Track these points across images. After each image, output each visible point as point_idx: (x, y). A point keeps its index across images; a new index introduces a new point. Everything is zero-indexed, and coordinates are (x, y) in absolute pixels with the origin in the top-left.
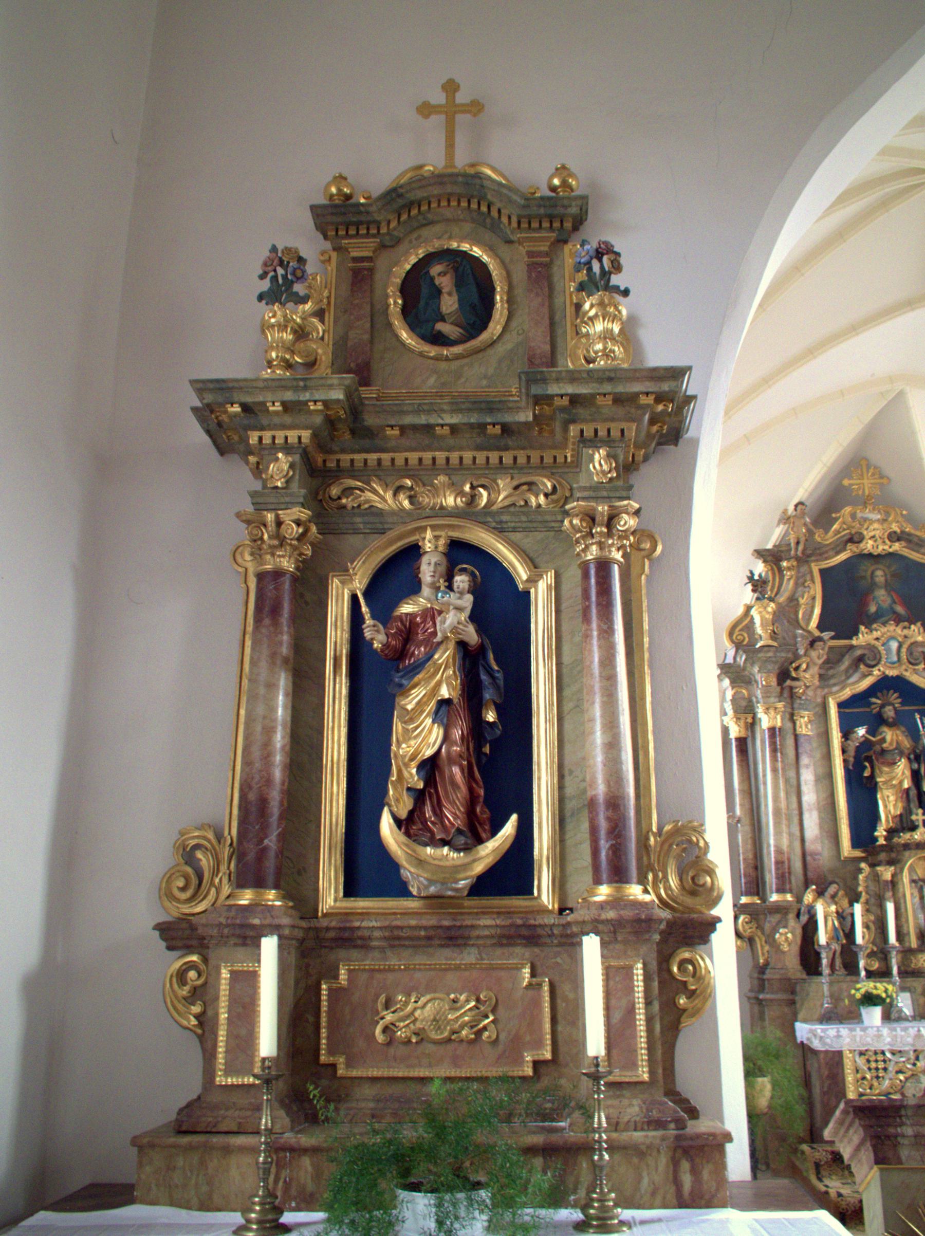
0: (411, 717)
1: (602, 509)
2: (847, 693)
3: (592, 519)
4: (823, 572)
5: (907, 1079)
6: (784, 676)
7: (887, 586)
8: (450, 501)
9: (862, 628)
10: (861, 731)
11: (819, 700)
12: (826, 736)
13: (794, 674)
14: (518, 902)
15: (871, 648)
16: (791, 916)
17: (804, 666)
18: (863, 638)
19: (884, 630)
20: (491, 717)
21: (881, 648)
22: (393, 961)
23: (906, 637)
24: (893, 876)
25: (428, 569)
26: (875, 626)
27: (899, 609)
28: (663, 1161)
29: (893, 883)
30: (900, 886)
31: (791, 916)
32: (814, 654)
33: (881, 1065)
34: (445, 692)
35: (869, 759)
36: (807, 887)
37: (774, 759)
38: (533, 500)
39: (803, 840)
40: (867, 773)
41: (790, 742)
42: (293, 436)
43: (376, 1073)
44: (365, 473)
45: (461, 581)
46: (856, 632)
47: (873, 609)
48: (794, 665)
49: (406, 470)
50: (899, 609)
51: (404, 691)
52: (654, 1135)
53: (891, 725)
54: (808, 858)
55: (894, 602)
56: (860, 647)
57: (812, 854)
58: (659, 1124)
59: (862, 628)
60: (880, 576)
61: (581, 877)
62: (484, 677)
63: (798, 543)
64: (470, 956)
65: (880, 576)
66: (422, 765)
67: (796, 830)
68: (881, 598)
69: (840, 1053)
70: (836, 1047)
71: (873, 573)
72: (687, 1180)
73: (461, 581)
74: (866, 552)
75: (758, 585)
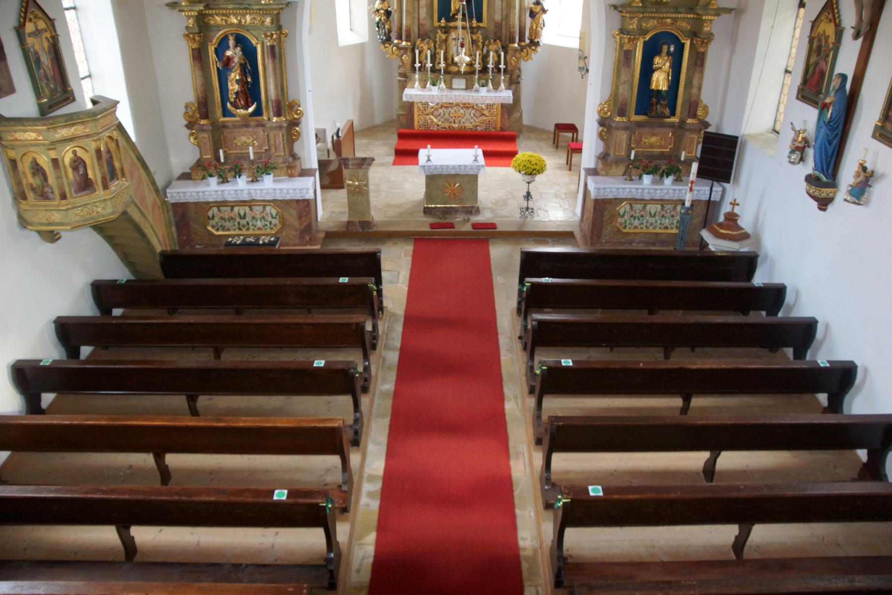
0: (231, 81)
1: (269, 34)
3: (266, 36)
8: (235, 21)
14: (260, 118)
20: (249, 80)
22: (235, 131)
24: (446, 37)
25: (231, 42)
28: (285, 170)
29: (446, 40)
30: (448, 43)
31: (409, 51)
33: (426, 106)
34: (238, 78)
36: (419, 38)
38: (256, 22)
39: (419, 19)
42: (193, 13)
43: (234, 152)
44: (212, 15)
45: (239, 49)
49: (223, 15)
51: (230, 75)
52: (283, 165)
58: (285, 163)
61: (271, 114)
62: (247, 71)
64: (250, 129)
66: (235, 93)
67: (416, 15)
69: (413, 103)
70: (411, 100)
72: (289, 172)
73: (239, 49)
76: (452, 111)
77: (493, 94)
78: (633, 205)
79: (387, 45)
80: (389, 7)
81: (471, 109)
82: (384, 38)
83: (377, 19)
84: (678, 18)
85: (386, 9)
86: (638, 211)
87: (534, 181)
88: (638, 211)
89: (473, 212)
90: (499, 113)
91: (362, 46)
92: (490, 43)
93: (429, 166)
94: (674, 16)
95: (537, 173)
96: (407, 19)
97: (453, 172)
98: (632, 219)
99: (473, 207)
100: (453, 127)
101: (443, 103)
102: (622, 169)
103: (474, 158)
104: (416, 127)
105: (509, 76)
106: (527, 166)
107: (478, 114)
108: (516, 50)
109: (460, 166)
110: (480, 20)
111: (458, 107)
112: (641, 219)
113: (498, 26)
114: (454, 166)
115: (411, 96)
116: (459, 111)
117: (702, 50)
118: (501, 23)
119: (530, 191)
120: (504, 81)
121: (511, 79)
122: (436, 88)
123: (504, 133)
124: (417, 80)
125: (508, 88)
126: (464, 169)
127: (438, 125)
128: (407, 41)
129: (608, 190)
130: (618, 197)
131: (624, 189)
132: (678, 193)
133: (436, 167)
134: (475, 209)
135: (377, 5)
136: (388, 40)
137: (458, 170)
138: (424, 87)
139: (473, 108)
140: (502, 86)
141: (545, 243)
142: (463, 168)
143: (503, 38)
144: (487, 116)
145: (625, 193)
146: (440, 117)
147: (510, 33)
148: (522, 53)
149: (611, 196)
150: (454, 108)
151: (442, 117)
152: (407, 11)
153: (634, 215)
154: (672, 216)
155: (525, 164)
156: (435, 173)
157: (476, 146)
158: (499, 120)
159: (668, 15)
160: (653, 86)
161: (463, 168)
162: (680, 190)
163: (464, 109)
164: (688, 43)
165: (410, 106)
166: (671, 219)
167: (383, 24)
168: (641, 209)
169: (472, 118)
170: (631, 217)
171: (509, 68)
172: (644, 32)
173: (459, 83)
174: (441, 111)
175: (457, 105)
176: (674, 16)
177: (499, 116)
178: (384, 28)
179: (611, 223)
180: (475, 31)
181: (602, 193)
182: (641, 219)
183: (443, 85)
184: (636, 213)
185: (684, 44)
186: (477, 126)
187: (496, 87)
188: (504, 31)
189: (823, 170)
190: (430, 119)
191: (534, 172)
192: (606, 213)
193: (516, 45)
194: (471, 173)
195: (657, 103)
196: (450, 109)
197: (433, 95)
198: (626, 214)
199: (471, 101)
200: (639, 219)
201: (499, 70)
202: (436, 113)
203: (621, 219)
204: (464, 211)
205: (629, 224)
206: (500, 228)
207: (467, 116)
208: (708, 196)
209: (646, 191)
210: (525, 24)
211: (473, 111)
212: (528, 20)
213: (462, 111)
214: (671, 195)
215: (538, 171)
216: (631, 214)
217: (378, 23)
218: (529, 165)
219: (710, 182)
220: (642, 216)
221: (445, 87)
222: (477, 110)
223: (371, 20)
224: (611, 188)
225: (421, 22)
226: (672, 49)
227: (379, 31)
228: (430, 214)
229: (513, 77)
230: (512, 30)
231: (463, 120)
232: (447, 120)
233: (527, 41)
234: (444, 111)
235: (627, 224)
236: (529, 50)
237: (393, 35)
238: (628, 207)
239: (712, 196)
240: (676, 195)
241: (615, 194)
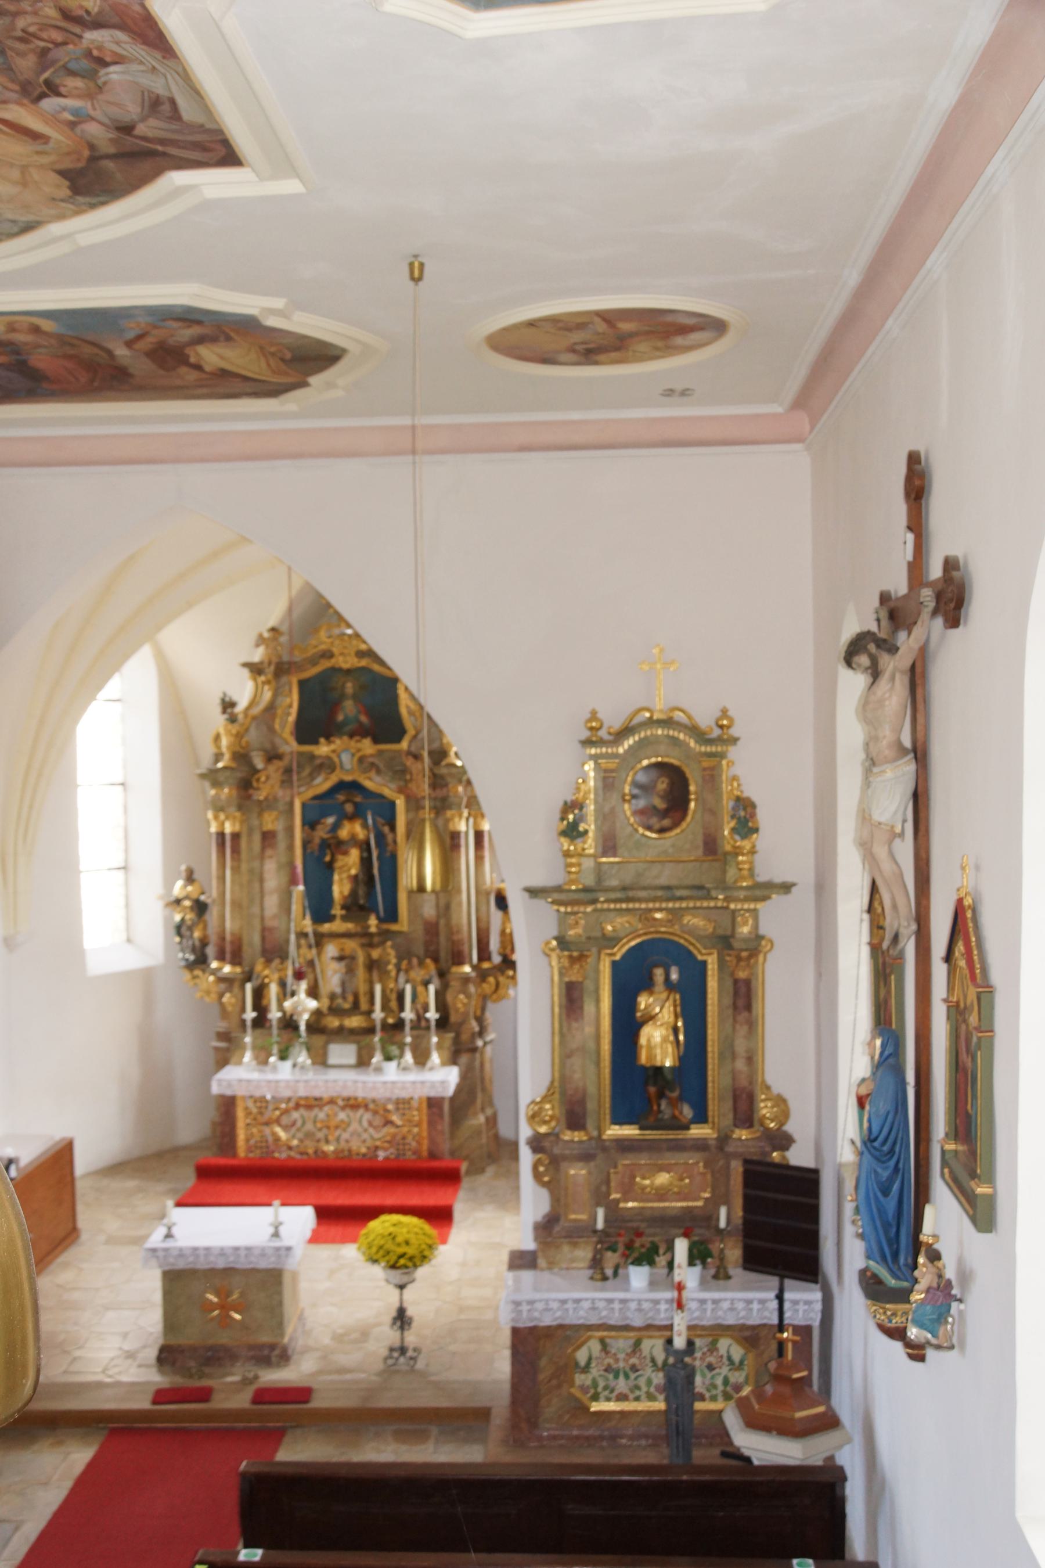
2: (311, 793)
4: (302, 684)
5: (282, 1114)
6: (246, 785)
7: (355, 697)
9: (322, 740)
10: (330, 820)
11: (288, 799)
12: (290, 830)
13: (255, 784)
15: (328, 758)
16: (236, 985)
17: (263, 779)
18: (323, 749)
19: (338, 742)
21: (336, 759)
23: (359, 750)
26: (332, 739)
27: (364, 719)
32: (271, 769)
35: (329, 846)
37: (233, 858)
39: (262, 918)
40: (328, 858)
41: (257, 838)
46: (316, 742)
47: (340, 717)
48: (256, 776)
50: (364, 719)
53: (351, 818)
54: (267, 933)
55: (359, 712)
56: (320, 757)
57: (271, 930)
59: (322, 740)
60: (349, 687)
63: (270, 663)
65: (349, 687)
67: (256, 910)
68: (349, 709)
71: (343, 687)
74: (337, 666)
75: (228, 705)
76: (322, 1115)
77: (414, 1076)
78: (608, 1341)
79: (197, 972)
80: (203, 893)
81: (361, 1111)
82: (192, 958)
83: (178, 918)
84: (681, 909)
85: (195, 896)
86: (621, 1356)
87: (413, 1281)
88: (621, 1356)
89: (274, 1359)
90: (425, 1118)
91: (146, 976)
92: (410, 967)
93: (166, 1250)
94: (670, 905)
95: (410, 1264)
96: (233, 918)
97: (221, 1264)
98: (611, 1376)
99: (272, 1347)
100: (323, 1152)
101: (301, 1098)
102: (584, 1253)
103: (271, 1230)
104: (242, 1151)
105: (451, 1035)
106: (385, 1247)
107: (378, 1121)
108: (466, 980)
109: (236, 1249)
110: (392, 915)
111: (336, 1109)
112: (633, 1376)
113: (432, 930)
114: (222, 1249)
115: (230, 1085)
116: (336, 1114)
117: (742, 975)
118: (437, 924)
119: (405, 1305)
120: (439, 1046)
121: (456, 1041)
122: (288, 1064)
123: (435, 1164)
124: (249, 1046)
125: (453, 1059)
126: (246, 1256)
127: (290, 1148)
128: (234, 963)
129: (540, 1306)
130: (567, 1322)
131: (577, 1301)
132: (713, 1310)
133: (181, 1253)
134: (277, 1352)
135: (179, 888)
136: (200, 961)
137: (232, 1259)
138: (262, 1061)
139: (366, 1107)
140: (435, 1058)
141: (420, 1437)
142: (243, 1253)
143: (443, 954)
144: (397, 1127)
145: (582, 1313)
146: (293, 1130)
147: (453, 943)
148: (485, 985)
149: (547, 1321)
150: (326, 1108)
151: (298, 1130)
152: (234, 903)
153: (615, 1366)
154: (710, 1367)
155: (382, 1242)
156: (181, 1265)
157: (277, 1203)
158: (425, 1134)
159: (657, 905)
160: (643, 1059)
161: (243, 1253)
162: (715, 1302)
163: (348, 1111)
164: (712, 962)
165: (228, 1105)
166: (709, 1375)
167: (190, 929)
168: (629, 1351)
169: (366, 1130)
170: (606, 1370)
171: (453, 1018)
172: (611, 941)
173: (342, 1053)
174: (295, 1115)
175: (332, 1101)
176: (670, 905)
177: (425, 1126)
178: (191, 937)
179: (559, 1386)
180: (376, 940)
181: (525, 1314)
182: (633, 1376)
183: (303, 1058)
184: (617, 1360)
185: (704, 963)
186: (377, 1148)
187: (421, 1059)
188: (442, 939)
189: (884, 1258)
190: (274, 1134)
191: (402, 1261)
192: (543, 1362)
193: (467, 969)
194: (263, 1264)
195: (661, 1095)
196: (316, 1111)
197: (277, 1082)
198: (593, 1365)
199: (360, 1094)
200: (627, 1377)
201: (400, 1025)
202: (285, 1120)
203: (583, 1376)
204: (253, 1358)
206: (317, 1403)
207: (354, 1126)
209: (633, 1305)
210: (488, 923)
211: (367, 1116)
212: (496, 915)
213: (342, 1116)
214: (743, 1314)
215: (411, 1259)
217: (179, 929)
218: (390, 1246)
219: (774, 1281)
220: (634, 1368)
221: (309, 1062)
222: (375, 1113)
223: (167, 919)
224: (547, 1301)
225: (269, 923)
226: (674, 976)
227: (180, 943)
228: (173, 1364)
229: (465, 1037)
230: (455, 938)
231: (345, 1136)
232: (309, 1135)
233: (497, 959)
234: (302, 1116)
235: (600, 1389)
236: (501, 979)
237: (210, 951)
238: (595, 1346)
239: (787, 1315)
240: (709, 1313)
241: (558, 1314)
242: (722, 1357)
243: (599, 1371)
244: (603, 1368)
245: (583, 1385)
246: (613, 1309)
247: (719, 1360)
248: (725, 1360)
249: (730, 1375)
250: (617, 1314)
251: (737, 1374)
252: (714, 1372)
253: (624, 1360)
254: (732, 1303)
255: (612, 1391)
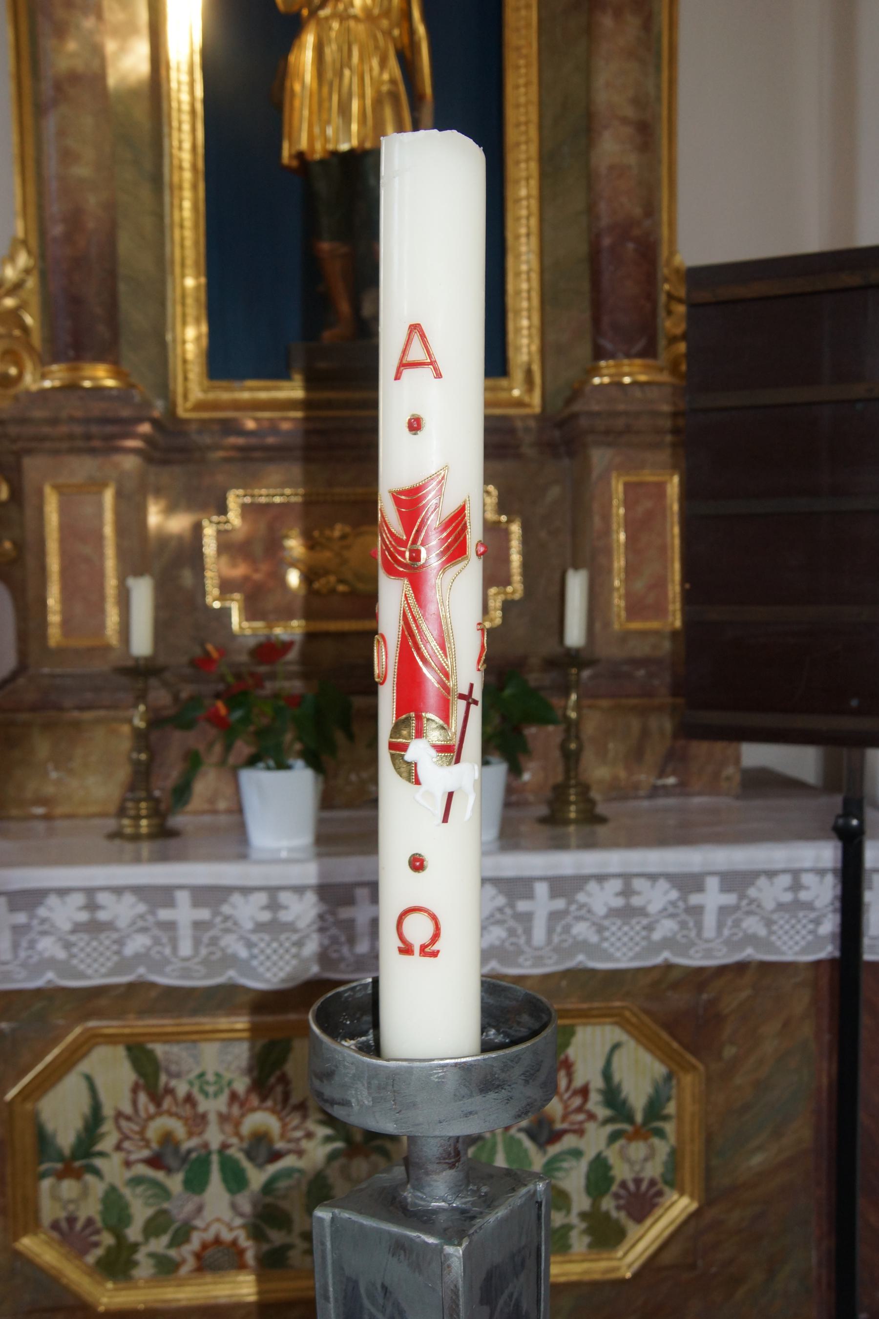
78: (159, 1049)
98: (175, 1183)
170: (154, 1162)
203: (69, 1188)
205: (153, 1228)
208: (830, 925)
216: (154, 1129)
235: (134, 1233)
240: (539, 933)
242: (584, 1092)
243: (128, 1164)
244: (146, 1153)
245: (71, 1220)
246: (170, 926)
247: (577, 1101)
248: (595, 1103)
249: (612, 1155)
250: (186, 948)
251: (638, 1150)
252: (554, 1150)
253: (223, 1118)
254: (627, 892)
255: (181, 1236)
